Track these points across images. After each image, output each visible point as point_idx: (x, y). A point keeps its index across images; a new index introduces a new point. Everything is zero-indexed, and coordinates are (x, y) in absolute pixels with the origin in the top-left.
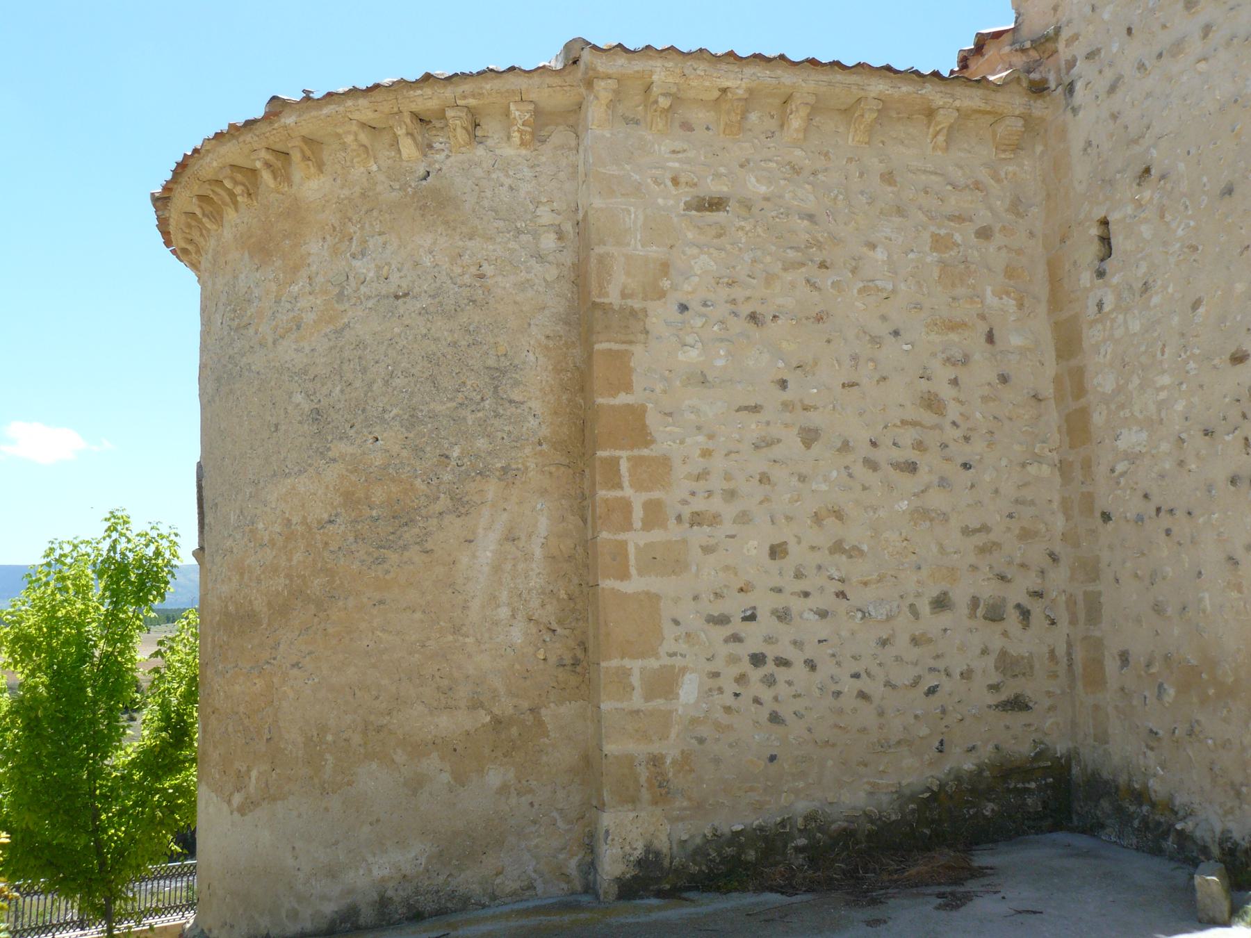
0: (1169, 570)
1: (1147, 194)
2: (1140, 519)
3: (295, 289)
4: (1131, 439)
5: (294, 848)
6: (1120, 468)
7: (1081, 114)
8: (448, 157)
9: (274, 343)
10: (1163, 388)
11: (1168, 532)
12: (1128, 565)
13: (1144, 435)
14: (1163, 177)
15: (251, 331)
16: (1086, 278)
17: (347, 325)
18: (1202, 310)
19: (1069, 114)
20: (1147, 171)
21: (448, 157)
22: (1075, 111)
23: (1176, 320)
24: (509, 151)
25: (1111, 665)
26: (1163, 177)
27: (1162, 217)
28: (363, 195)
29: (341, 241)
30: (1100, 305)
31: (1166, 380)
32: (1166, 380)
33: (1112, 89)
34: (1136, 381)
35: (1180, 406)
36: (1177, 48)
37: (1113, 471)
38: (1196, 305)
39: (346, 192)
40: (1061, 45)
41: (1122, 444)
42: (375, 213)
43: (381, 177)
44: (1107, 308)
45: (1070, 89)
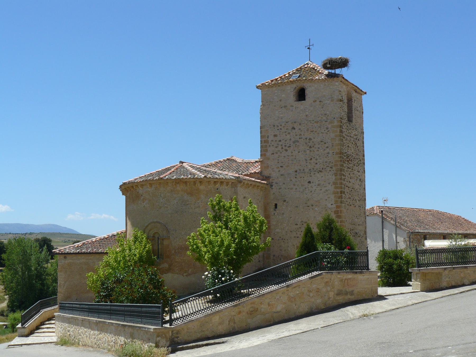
0: (283, 246)
1: (285, 203)
2: (279, 240)
3: (198, 201)
4: (277, 230)
5: (199, 280)
6: (275, 234)
7: (273, 189)
8: (220, 187)
9: (195, 209)
10: (285, 226)
11: (284, 241)
12: (276, 245)
13: (280, 230)
14: (287, 202)
15: (189, 206)
16: (272, 210)
17: (207, 208)
18: (291, 218)
19: (271, 189)
20: (285, 201)
21: (220, 187)
22: (272, 189)
23: (287, 218)
24: (226, 187)
25: (272, 257)
26: (287, 202)
27: (287, 207)
28: (210, 190)
29: (207, 196)
30: (274, 214)
31: (285, 225)
32: (285, 225)
33: (280, 189)
34: (280, 224)
35: (287, 228)
36: (292, 189)
37: (274, 234)
38: (291, 218)
39: (207, 189)
40: (271, 179)
41: (276, 231)
42: (212, 193)
43: (212, 188)
44: (276, 214)
45: (272, 186)
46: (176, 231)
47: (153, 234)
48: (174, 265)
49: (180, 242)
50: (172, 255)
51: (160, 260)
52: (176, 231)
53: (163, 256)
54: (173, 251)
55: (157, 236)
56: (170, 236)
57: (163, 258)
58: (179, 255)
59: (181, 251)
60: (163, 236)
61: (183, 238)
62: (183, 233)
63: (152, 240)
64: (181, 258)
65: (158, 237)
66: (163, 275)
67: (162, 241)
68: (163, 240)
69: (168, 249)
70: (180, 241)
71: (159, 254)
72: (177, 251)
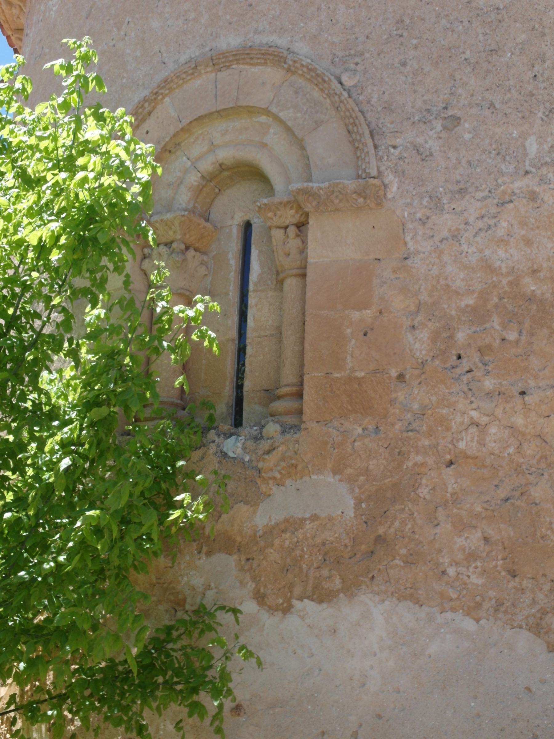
46: (457, 120)
47: (194, 179)
48: (424, 492)
49: (503, 242)
50: (401, 377)
51: (257, 439)
52: (457, 120)
53: (300, 395)
54: (424, 335)
55: (239, 218)
56: (389, 177)
57: (300, 412)
58: (489, 384)
59: (512, 336)
60: (310, 180)
61: (533, 196)
62: (532, 146)
63: (187, 248)
64: (519, 421)
65: (248, 227)
66: (287, 609)
67: (294, 243)
68: (301, 226)
69: (356, 315)
70: (501, 232)
71: (248, 385)
72: (461, 336)
